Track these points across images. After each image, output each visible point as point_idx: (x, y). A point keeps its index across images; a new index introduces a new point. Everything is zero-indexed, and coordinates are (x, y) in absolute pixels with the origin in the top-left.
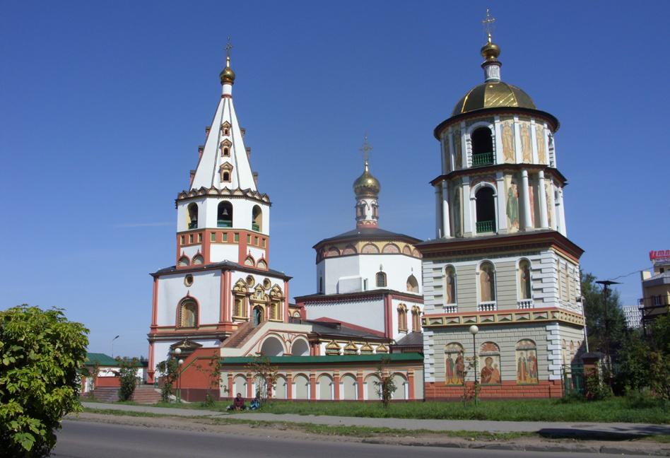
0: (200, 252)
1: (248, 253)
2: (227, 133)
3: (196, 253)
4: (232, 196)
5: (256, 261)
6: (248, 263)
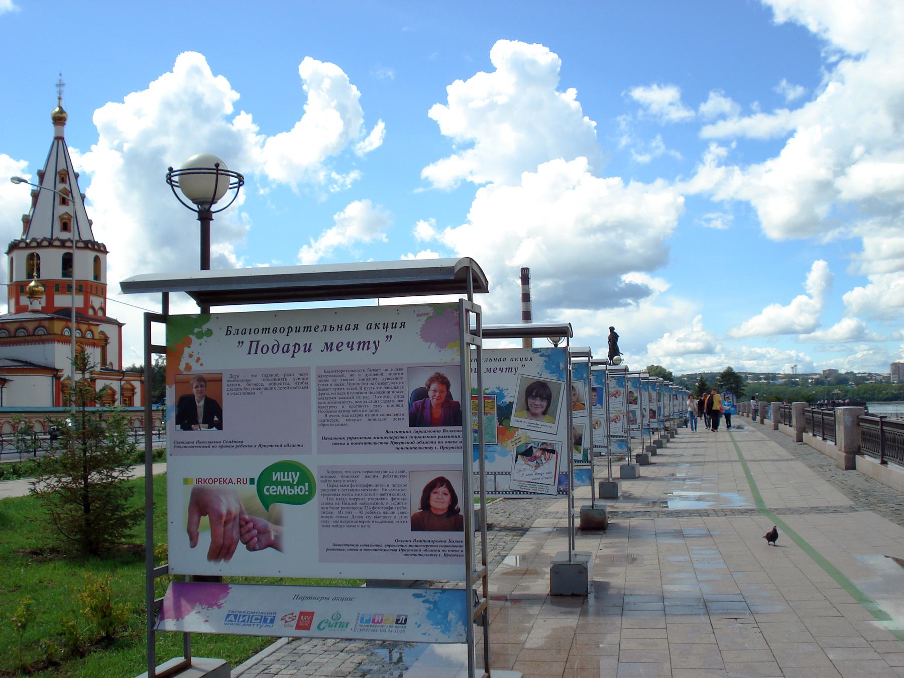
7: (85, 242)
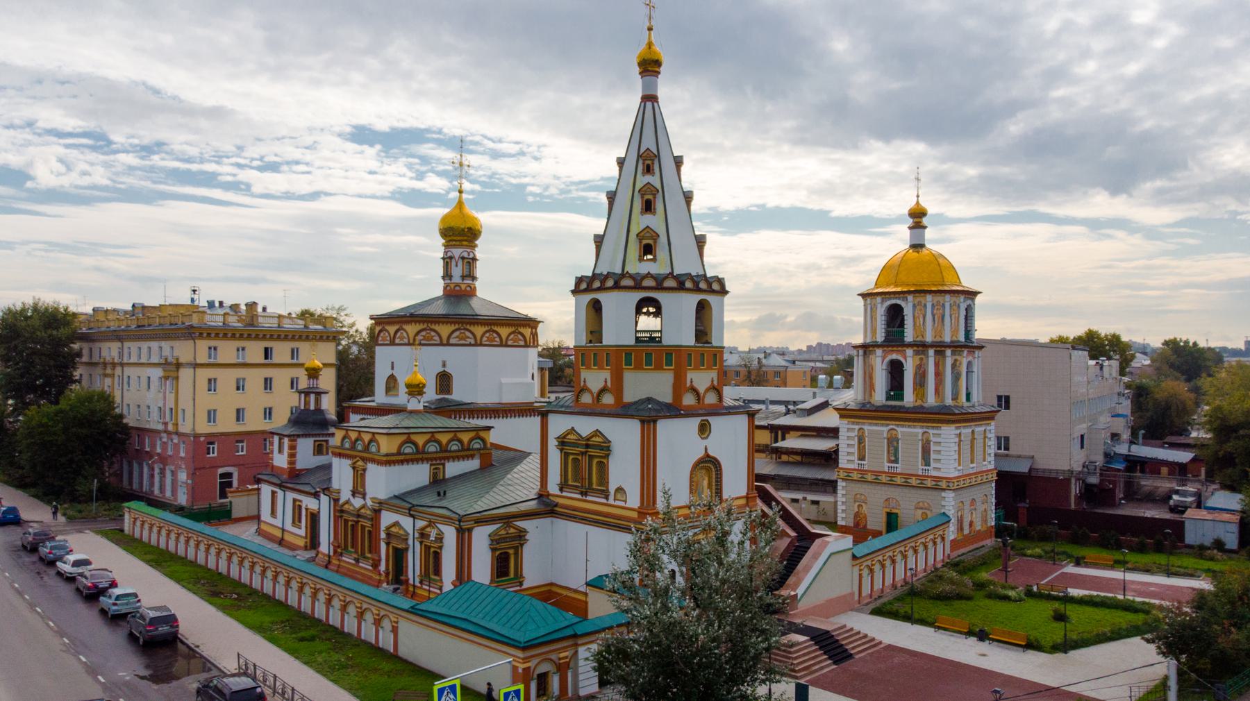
0: (609, 384)
1: (688, 384)
2: (648, 170)
3: (601, 385)
4: (659, 287)
5: (702, 391)
7: (676, 278)
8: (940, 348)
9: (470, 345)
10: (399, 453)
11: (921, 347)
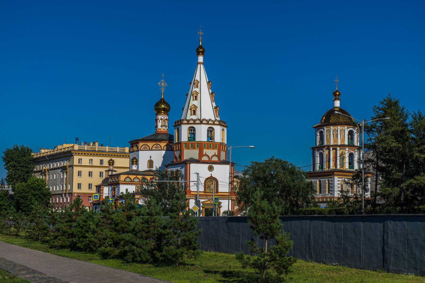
1: (204, 153)
4: (194, 123)
5: (210, 156)
6: (205, 158)
8: (335, 147)
9: (159, 150)
10: (125, 181)
11: (328, 147)
